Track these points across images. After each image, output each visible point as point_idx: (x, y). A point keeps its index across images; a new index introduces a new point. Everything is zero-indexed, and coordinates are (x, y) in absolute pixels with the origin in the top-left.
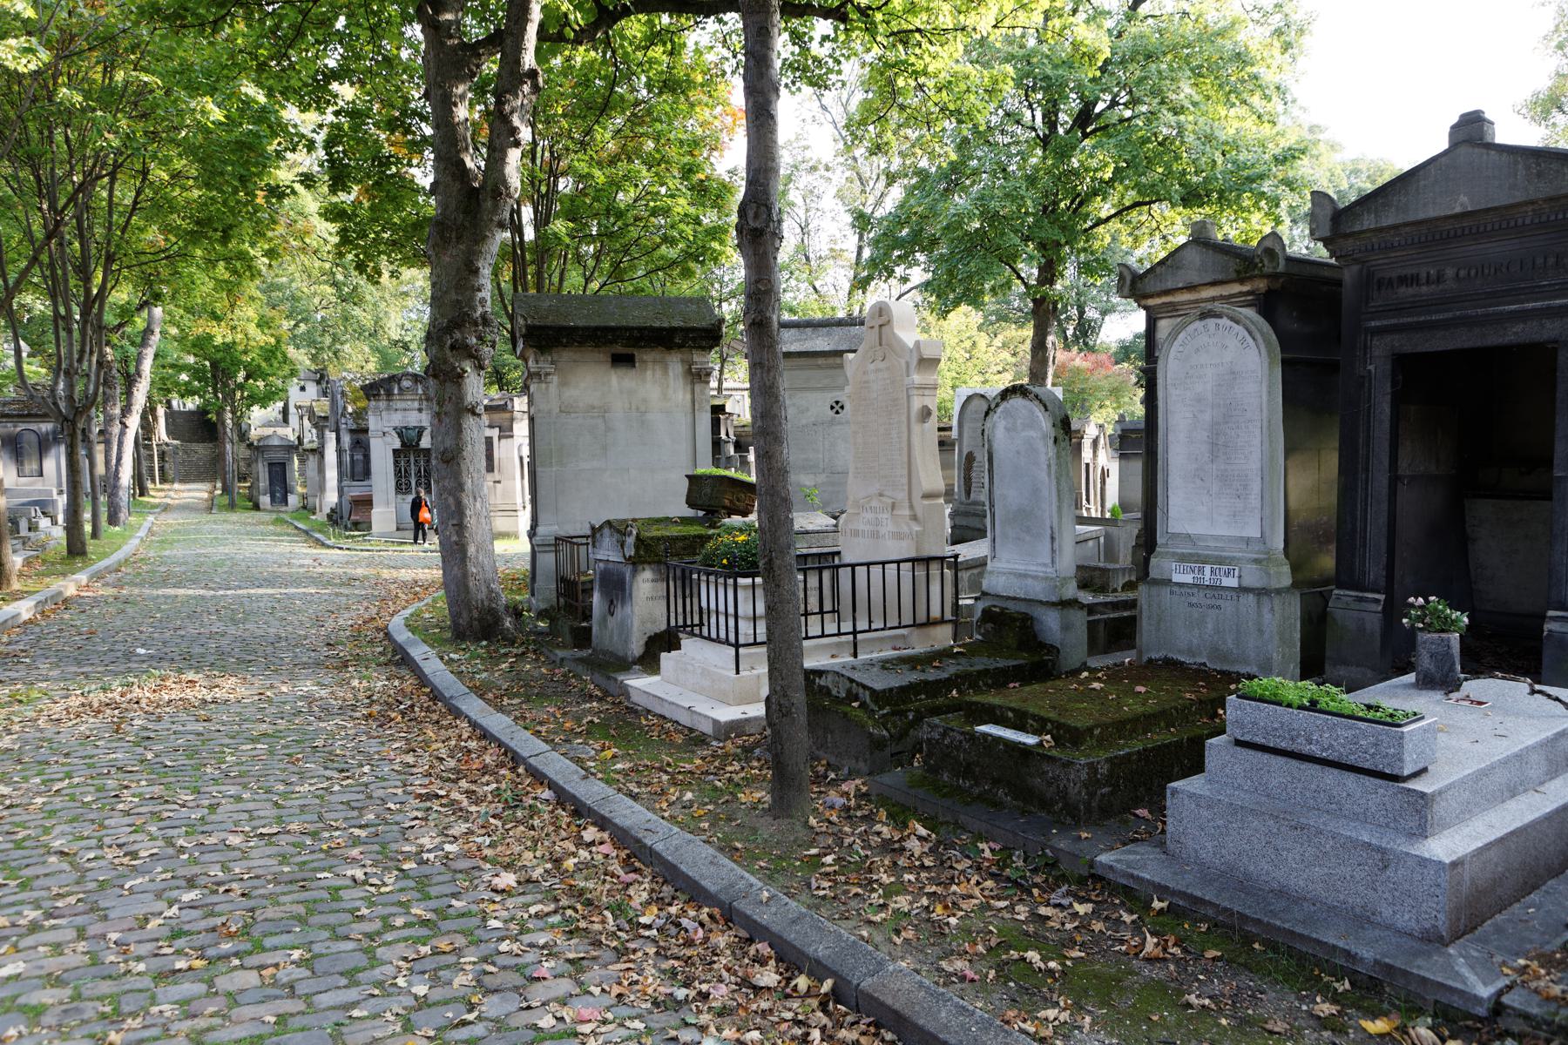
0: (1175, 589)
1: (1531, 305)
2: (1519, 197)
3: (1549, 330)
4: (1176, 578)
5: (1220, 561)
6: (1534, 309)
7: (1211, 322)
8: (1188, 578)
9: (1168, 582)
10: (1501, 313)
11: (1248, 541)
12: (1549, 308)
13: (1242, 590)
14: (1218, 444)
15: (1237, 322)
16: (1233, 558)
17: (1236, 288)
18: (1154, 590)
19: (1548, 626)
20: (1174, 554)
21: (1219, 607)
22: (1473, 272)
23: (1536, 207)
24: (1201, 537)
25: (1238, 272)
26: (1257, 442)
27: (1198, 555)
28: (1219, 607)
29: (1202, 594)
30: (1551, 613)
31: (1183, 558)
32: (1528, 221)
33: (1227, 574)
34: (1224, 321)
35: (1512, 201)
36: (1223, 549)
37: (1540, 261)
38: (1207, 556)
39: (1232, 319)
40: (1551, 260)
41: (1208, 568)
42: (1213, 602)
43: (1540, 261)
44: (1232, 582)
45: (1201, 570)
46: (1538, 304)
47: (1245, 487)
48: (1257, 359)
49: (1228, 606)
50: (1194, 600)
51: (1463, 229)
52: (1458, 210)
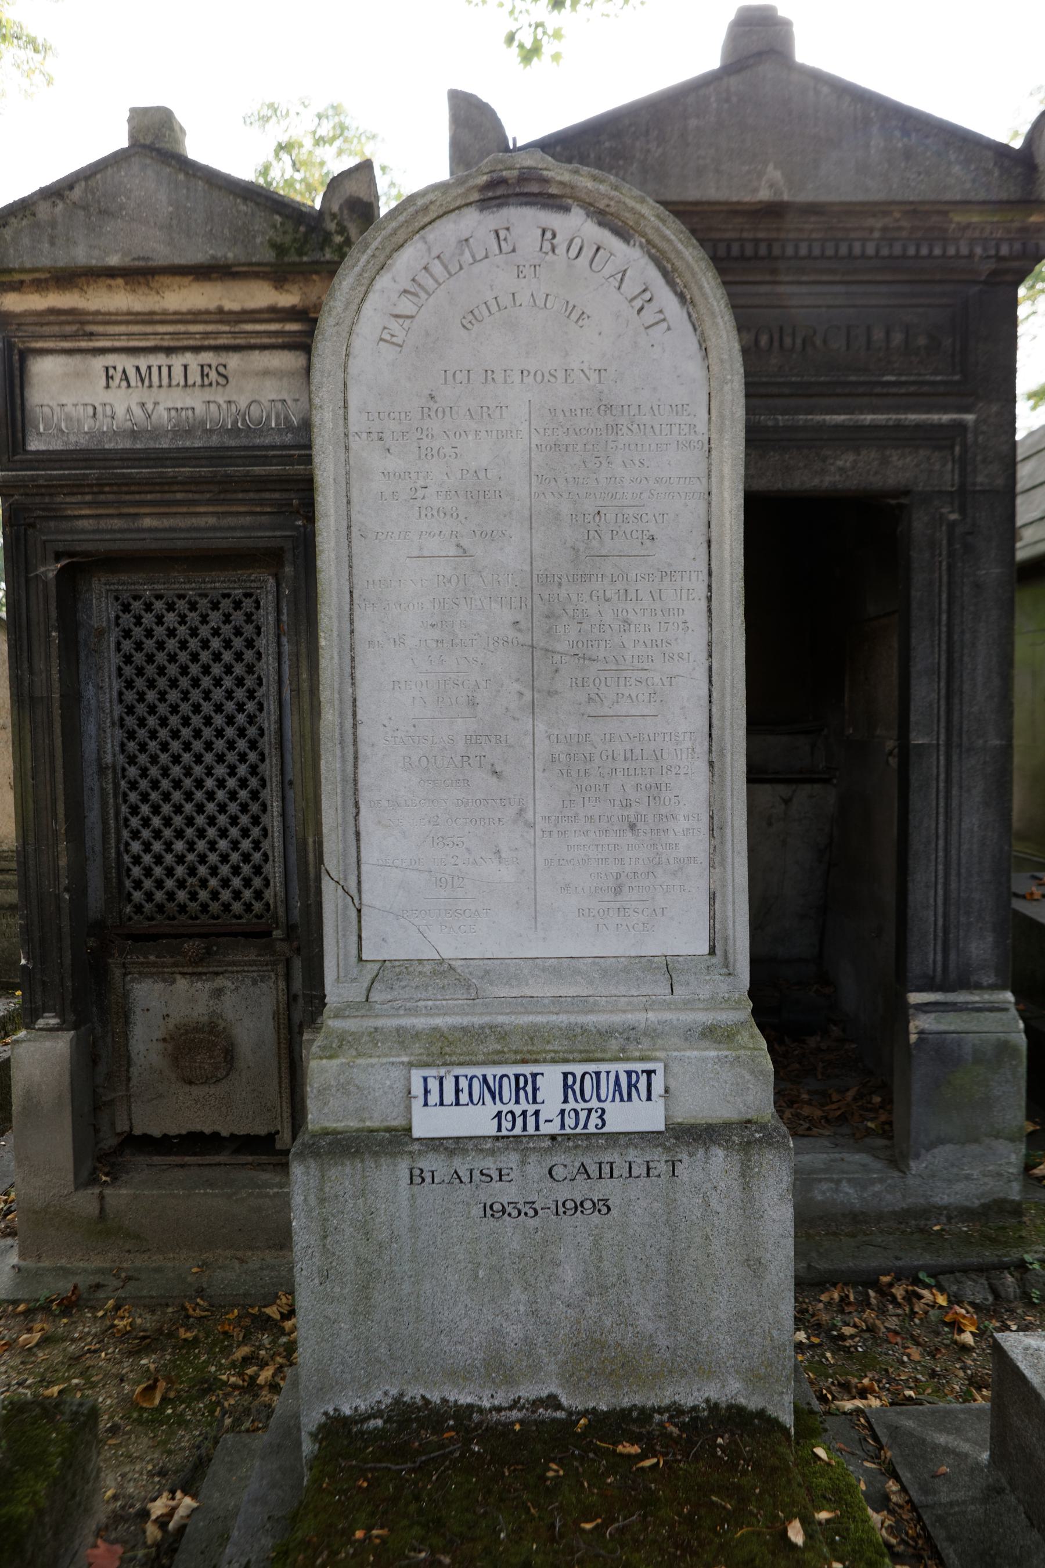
0: (429, 1163)
1: (868, 418)
2: (874, 191)
3: (898, 470)
4: (429, 1123)
5: (585, 1045)
6: (874, 427)
7: (525, 221)
8: (477, 1120)
9: (398, 1139)
10: (821, 427)
11: (669, 969)
12: (898, 427)
13: (687, 1136)
14: (554, 645)
15: (623, 233)
16: (630, 1034)
17: (261, 296)
18: (344, 1176)
19: (919, 1023)
20: (403, 1037)
21: (603, 1206)
22: (764, 340)
23: (887, 221)
24: (493, 969)
25: (280, 249)
26: (692, 643)
27: (502, 1034)
28: (603, 1206)
29: (535, 1168)
30: (915, 998)
31: (443, 1049)
32: (870, 250)
33: (626, 1090)
34: (575, 224)
35: (861, 197)
36: (583, 1004)
37: (878, 335)
38: (532, 1034)
39: (603, 217)
40: (898, 338)
41: (551, 1079)
42: (581, 1190)
43: (878, 335)
44: (644, 1115)
45: (527, 1087)
46: (880, 418)
47: (655, 793)
48: (694, 368)
49: (635, 1199)
50: (505, 1193)
51: (756, 241)
52: (764, 195)
